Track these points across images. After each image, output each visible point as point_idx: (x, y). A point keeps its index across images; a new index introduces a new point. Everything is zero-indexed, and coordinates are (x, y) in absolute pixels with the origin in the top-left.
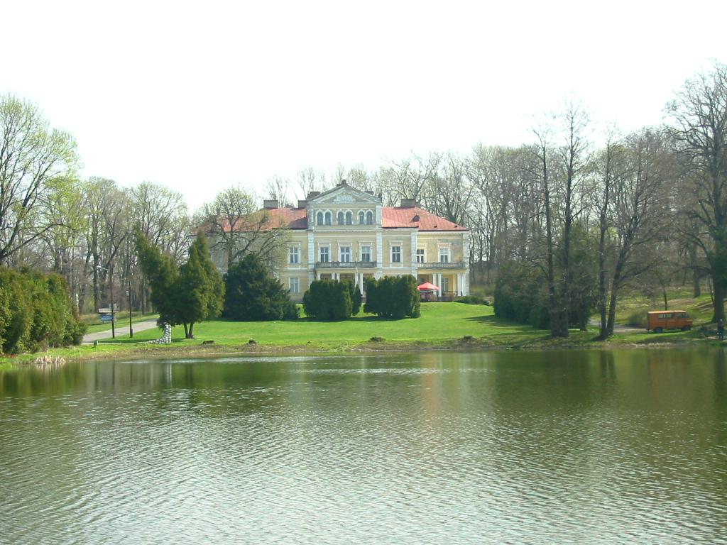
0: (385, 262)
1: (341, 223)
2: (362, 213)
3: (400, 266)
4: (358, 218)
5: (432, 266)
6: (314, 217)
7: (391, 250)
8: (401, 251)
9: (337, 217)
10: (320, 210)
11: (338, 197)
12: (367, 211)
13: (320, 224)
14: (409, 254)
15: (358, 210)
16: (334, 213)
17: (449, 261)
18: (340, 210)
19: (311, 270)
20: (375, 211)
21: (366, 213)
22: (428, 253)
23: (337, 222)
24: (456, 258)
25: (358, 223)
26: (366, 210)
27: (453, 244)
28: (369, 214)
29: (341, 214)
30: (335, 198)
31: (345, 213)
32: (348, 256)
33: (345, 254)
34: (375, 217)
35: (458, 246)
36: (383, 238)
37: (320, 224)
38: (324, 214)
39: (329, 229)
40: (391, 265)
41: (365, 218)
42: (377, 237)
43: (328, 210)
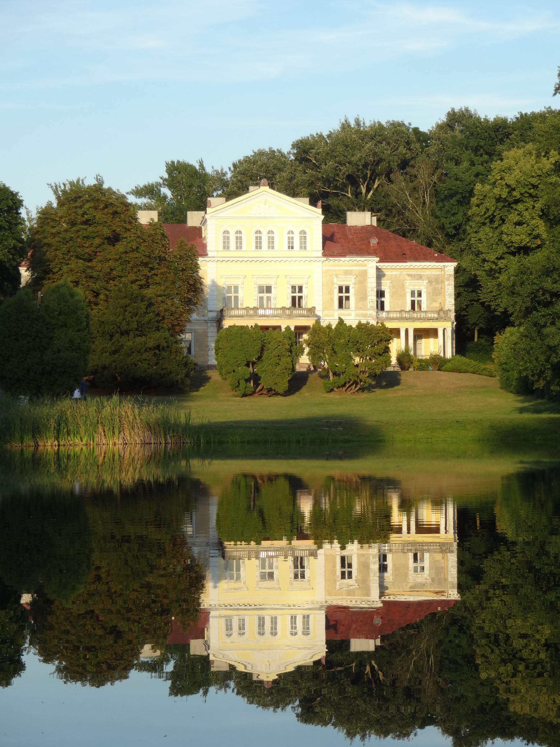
0: (327, 306)
1: (258, 246)
3: (351, 315)
5: (398, 315)
7: (337, 290)
8: (351, 290)
13: (226, 247)
14: (363, 297)
17: (424, 307)
19: (212, 320)
22: (391, 296)
24: (436, 305)
27: (430, 282)
32: (269, 299)
33: (265, 295)
35: (439, 286)
36: (325, 273)
37: (226, 247)
39: (239, 254)
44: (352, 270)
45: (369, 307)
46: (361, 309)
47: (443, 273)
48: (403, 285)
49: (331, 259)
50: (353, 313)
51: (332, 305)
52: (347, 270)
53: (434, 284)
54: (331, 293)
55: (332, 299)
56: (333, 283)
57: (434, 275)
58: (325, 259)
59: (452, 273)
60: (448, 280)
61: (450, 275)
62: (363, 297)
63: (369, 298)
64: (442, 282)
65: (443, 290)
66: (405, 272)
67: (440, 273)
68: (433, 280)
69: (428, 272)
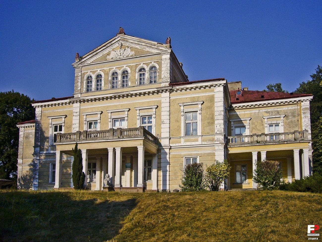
2: (142, 69)
3: (198, 141)
4: (137, 76)
6: (82, 83)
7: (183, 118)
9: (110, 78)
10: (89, 73)
11: (113, 53)
12: (151, 65)
15: (136, 66)
16: (107, 74)
18: (114, 69)
20: (160, 64)
21: (147, 69)
23: (110, 86)
25: (137, 83)
26: (147, 64)
28: (152, 68)
29: (114, 74)
30: (109, 54)
31: (120, 72)
34: (160, 73)
38: (94, 77)
40: (182, 140)
41: (147, 75)
42: (163, 100)
43: (99, 72)
44: (199, 97)
45: (216, 131)
46: (208, 134)
47: (299, 107)
48: (262, 121)
49: (178, 87)
50: (200, 139)
51: (180, 132)
52: (194, 97)
53: (291, 117)
54: (178, 121)
55: (179, 127)
56: (180, 111)
57: (290, 109)
58: (171, 88)
59: (309, 107)
60: (304, 113)
61: (306, 109)
62: (210, 121)
63: (216, 122)
64: (299, 115)
65: (299, 122)
66: (264, 110)
67: (296, 108)
68: (290, 114)
69: (285, 108)
